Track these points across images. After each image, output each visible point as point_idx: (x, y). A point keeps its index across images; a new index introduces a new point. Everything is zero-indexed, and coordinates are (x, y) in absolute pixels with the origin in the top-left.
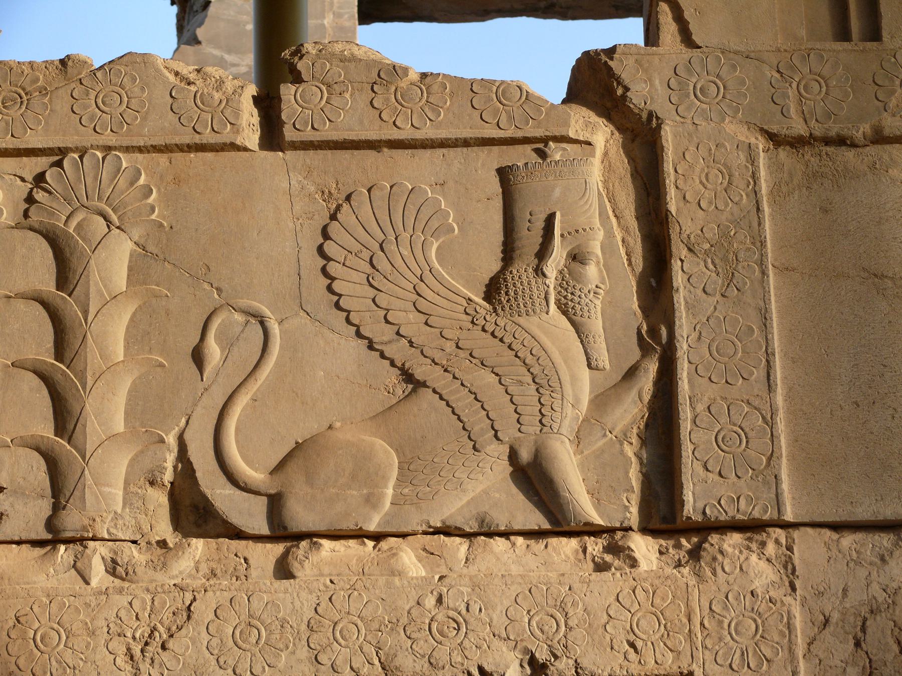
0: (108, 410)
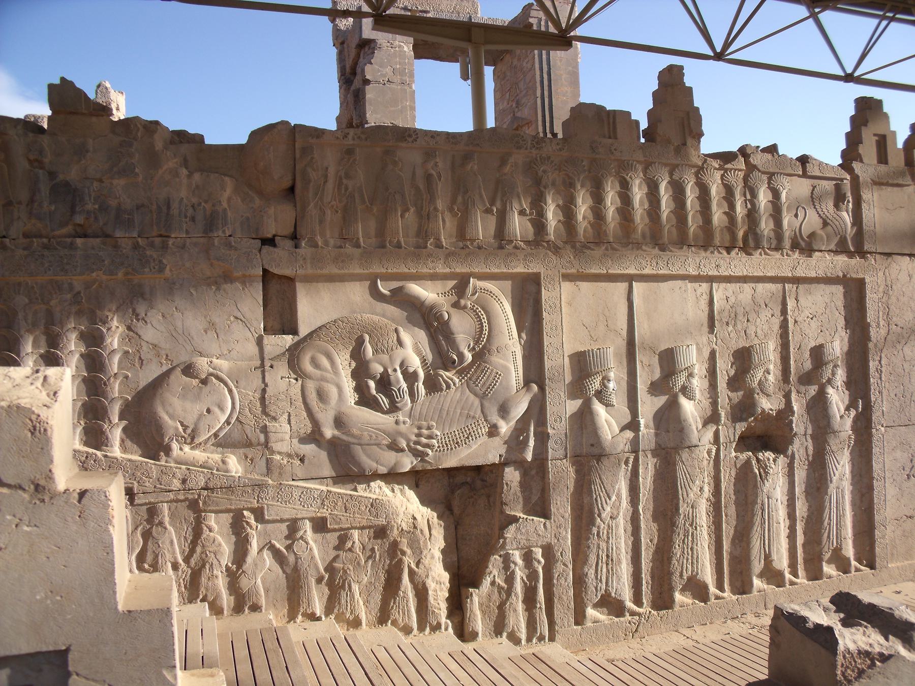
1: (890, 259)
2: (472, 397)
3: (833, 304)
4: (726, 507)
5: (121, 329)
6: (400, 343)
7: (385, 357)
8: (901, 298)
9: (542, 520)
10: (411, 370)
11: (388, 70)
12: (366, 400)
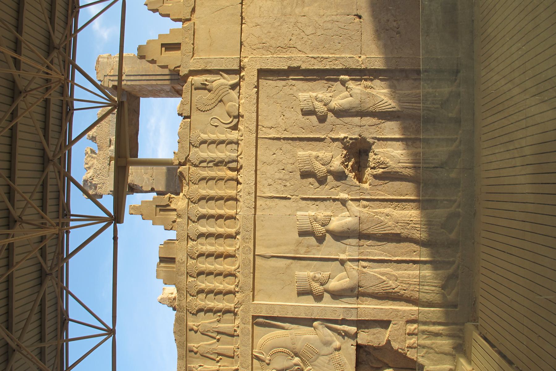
0: (222, 137)
1: (245, 43)
2: (318, 360)
3: (275, 97)
4: (401, 195)
8: (272, 34)
9: (391, 325)
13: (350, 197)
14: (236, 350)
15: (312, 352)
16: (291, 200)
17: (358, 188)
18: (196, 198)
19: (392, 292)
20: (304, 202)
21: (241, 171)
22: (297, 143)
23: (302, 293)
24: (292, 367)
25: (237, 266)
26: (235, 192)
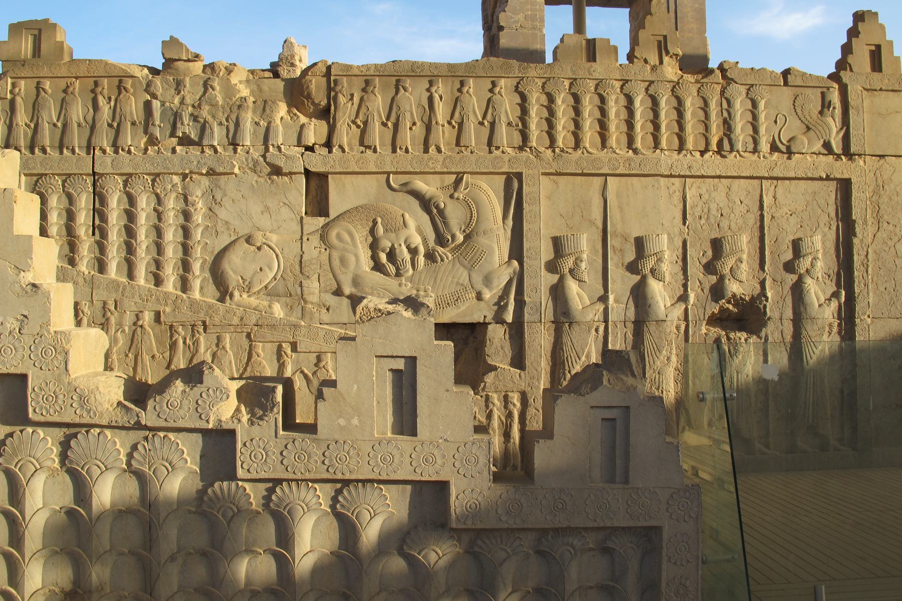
0: (762, 130)
1: (882, 161)
2: (462, 269)
3: (815, 203)
5: (204, 210)
6: (405, 224)
7: (392, 236)
8: (895, 198)
10: (413, 246)
11: (521, 17)
12: (378, 267)
13: (689, 307)
14: (469, 150)
15: (475, 259)
16: (682, 226)
17: (702, 318)
18: (679, 92)
19: (564, 369)
20: (681, 245)
21: (719, 157)
22: (757, 234)
23: (557, 243)
24: (449, 230)
25: (590, 150)
26: (691, 148)
